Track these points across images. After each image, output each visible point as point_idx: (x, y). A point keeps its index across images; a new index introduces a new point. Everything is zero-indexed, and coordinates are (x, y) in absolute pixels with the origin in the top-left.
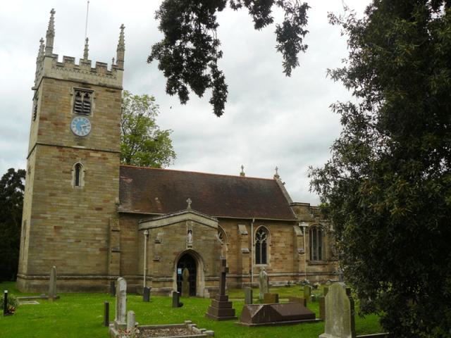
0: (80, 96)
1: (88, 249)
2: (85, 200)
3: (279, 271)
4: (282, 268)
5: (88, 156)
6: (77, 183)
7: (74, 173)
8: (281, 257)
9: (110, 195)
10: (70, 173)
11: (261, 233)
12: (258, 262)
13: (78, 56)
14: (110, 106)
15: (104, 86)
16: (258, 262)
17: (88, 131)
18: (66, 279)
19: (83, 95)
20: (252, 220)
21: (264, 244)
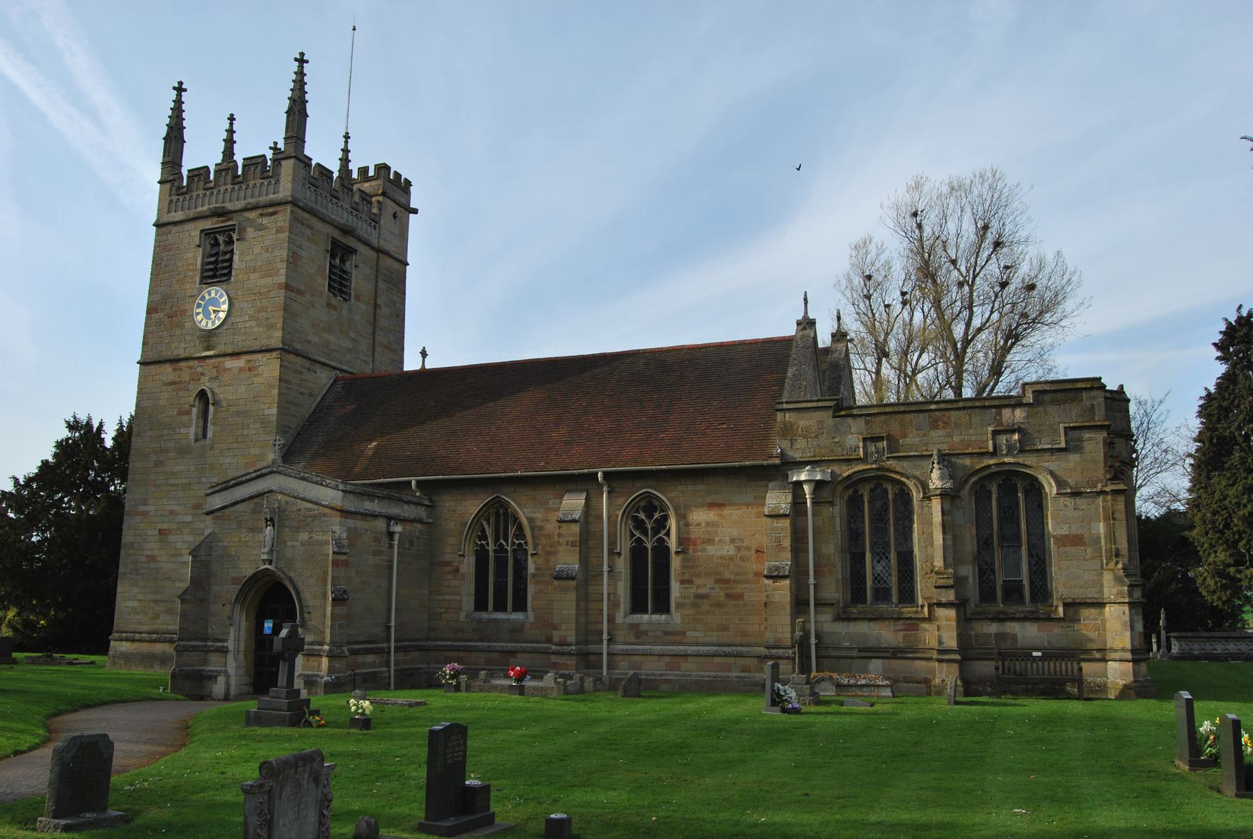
3: (715, 640)
6: (205, 436)
8: (719, 593)
10: (189, 413)
12: (638, 605)
16: (638, 605)
17: (222, 315)
21: (662, 551)
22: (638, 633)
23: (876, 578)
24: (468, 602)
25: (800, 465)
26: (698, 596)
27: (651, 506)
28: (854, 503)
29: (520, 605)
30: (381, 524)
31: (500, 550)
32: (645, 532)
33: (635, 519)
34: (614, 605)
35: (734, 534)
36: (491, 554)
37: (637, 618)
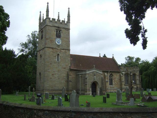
0: (58, 32)
1: (62, 81)
2: (60, 65)
4: (117, 87)
5: (61, 51)
7: (57, 56)
9: (68, 64)
10: (56, 57)
11: (111, 75)
12: (110, 85)
13: (56, 18)
14: (67, 35)
16: (110, 85)
18: (56, 91)
19: (58, 31)
21: (112, 79)
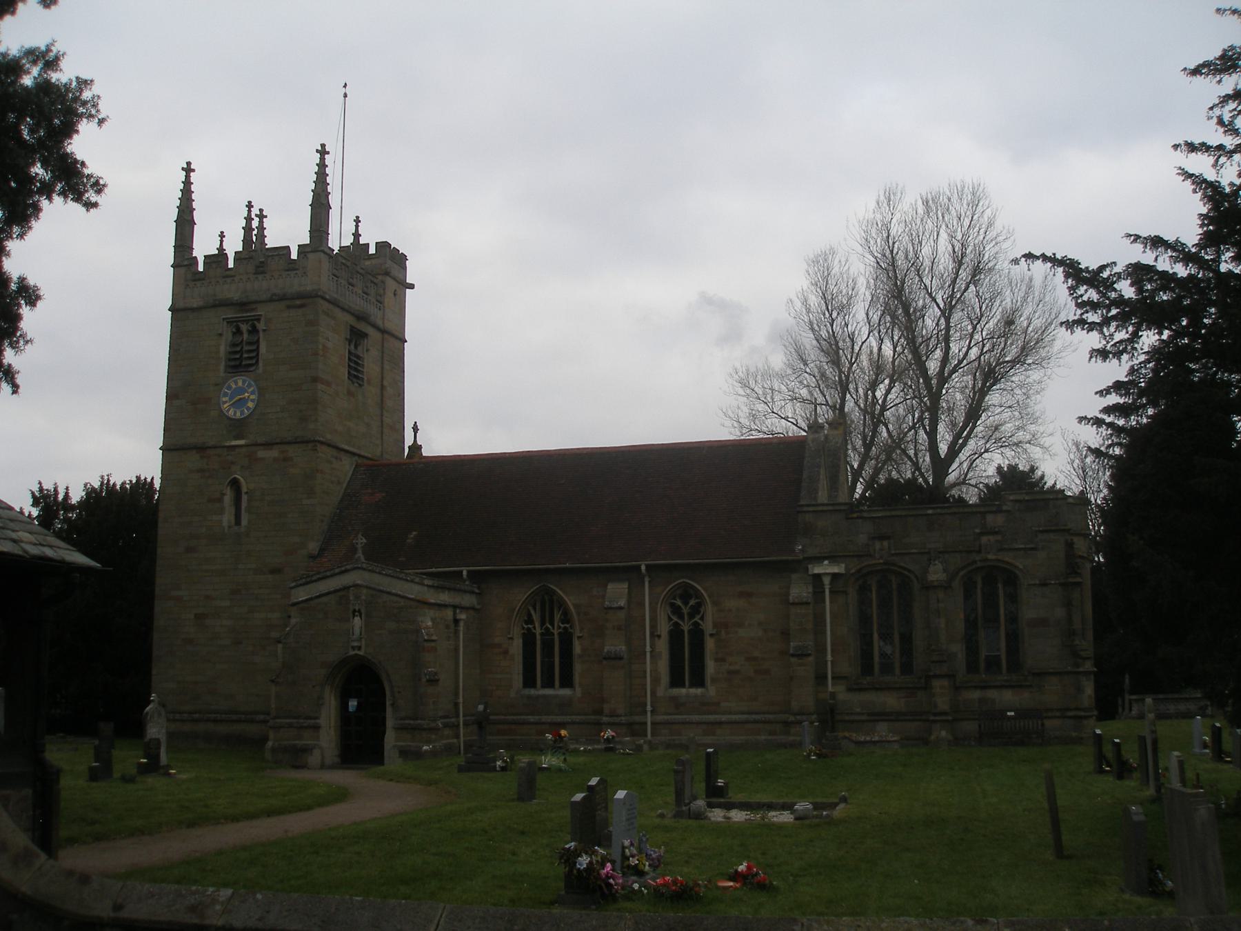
0: (241, 333)
6: (238, 521)
7: (228, 498)
10: (220, 500)
11: (686, 602)
12: (676, 681)
15: (282, 298)
16: (676, 681)
18: (215, 721)
20: (639, 567)
22: (677, 704)
23: (883, 655)
24: (518, 680)
25: (819, 559)
26: (729, 672)
27: (687, 593)
28: (863, 590)
29: (567, 681)
30: (449, 613)
31: (547, 632)
32: (681, 617)
33: (672, 605)
34: (656, 681)
35: (741, 617)
36: (538, 637)
37: (676, 691)
